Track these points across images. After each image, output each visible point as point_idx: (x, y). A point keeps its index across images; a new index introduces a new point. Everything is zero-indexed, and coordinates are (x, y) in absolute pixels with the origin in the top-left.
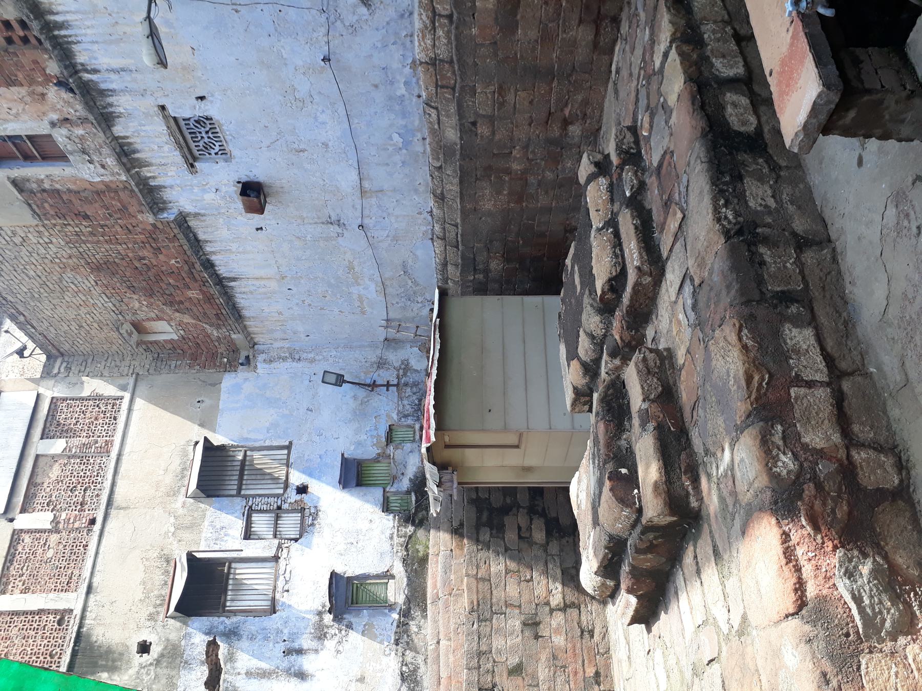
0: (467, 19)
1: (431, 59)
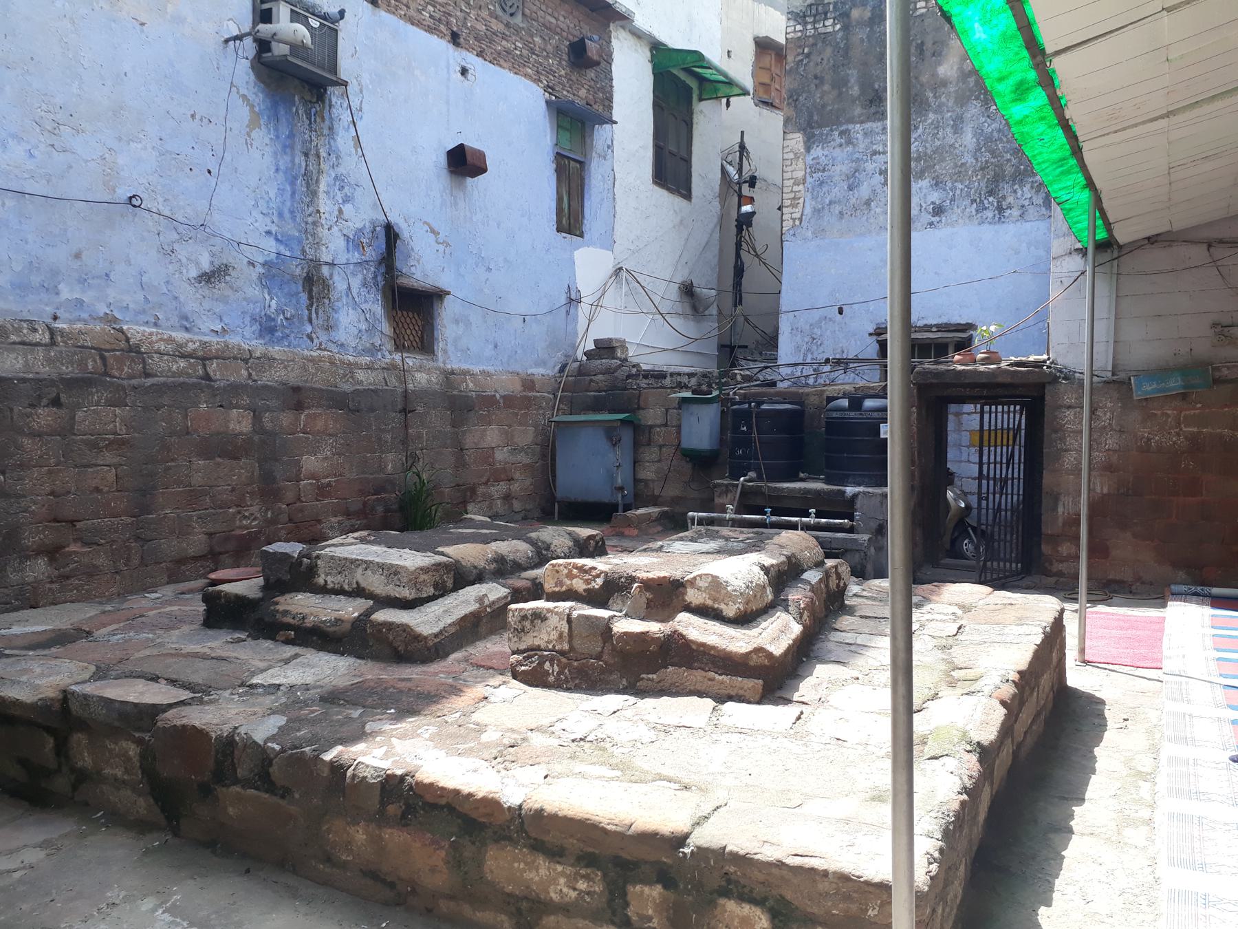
0: (218, 398)
1: (138, 346)
